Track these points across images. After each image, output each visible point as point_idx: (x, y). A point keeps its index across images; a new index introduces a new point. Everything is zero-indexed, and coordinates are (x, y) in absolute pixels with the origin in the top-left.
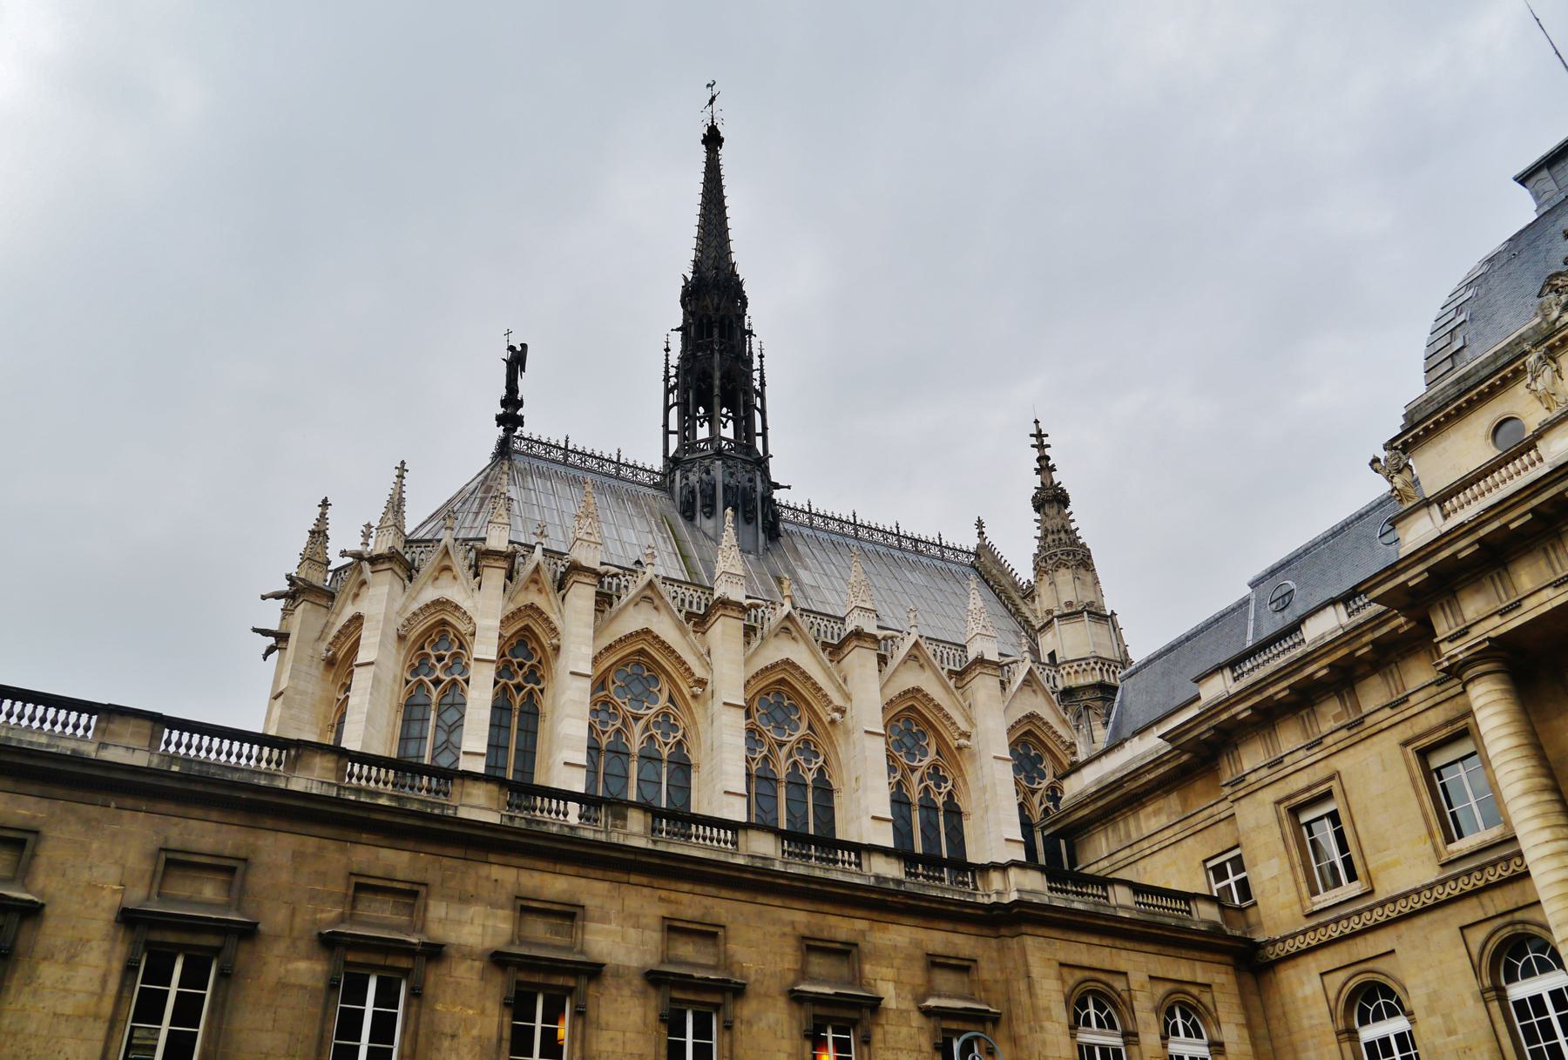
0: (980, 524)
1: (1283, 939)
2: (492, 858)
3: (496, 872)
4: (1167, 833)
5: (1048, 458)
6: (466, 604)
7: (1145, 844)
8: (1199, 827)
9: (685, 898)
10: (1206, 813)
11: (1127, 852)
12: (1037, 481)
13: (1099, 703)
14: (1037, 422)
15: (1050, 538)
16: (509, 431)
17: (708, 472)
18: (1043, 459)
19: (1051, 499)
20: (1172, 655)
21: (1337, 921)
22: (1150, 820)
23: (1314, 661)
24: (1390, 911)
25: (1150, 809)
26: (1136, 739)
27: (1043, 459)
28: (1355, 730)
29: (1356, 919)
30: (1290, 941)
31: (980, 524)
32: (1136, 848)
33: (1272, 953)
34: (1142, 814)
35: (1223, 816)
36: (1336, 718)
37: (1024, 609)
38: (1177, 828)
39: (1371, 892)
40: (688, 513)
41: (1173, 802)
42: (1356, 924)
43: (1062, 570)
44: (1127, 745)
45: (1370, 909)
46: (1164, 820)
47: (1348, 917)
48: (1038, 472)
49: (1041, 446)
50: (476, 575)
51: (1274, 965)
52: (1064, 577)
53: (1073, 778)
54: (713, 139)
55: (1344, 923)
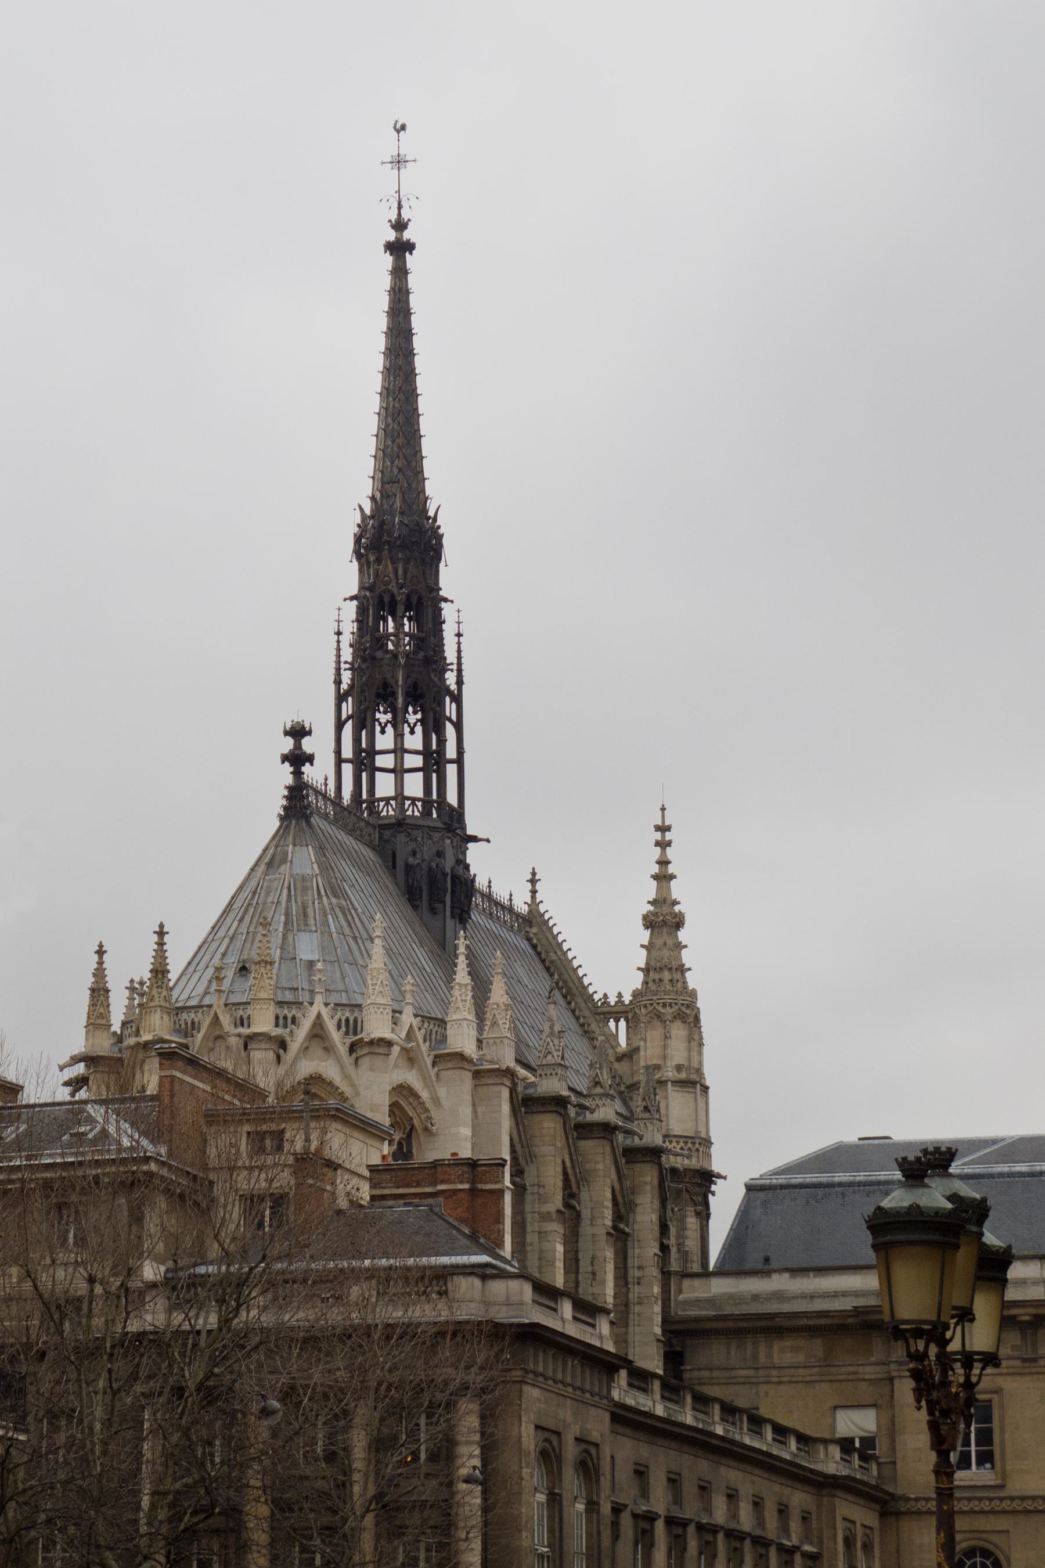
0: (533, 881)
1: (917, 1500)
2: (723, 1461)
3: (723, 1471)
4: (801, 1371)
5: (669, 862)
6: (425, 1095)
7: (774, 1372)
8: (840, 1377)
9: (756, 1479)
10: (851, 1369)
11: (752, 1372)
12: (651, 889)
13: (697, 1189)
14: (663, 809)
15: (666, 975)
16: (297, 773)
17: (440, 854)
18: (663, 863)
19: (664, 921)
20: (820, 1191)
21: (969, 1499)
22: (785, 1353)
23: (1023, 1307)
24: (1017, 1505)
25: (788, 1343)
26: (787, 1275)
27: (663, 863)
28: (1027, 1365)
29: (987, 1503)
30: (923, 1503)
31: (533, 881)
32: (761, 1372)
33: (902, 1506)
34: (777, 1345)
35: (867, 1377)
36: (1013, 1348)
37: (594, 1027)
38: (816, 1370)
39: (1002, 1487)
40: (412, 895)
41: (817, 1346)
42: (986, 1505)
43: (678, 1023)
44: (775, 1277)
45: (1001, 1499)
46: (800, 1358)
47: (980, 1499)
48: (655, 877)
49: (663, 845)
50: (434, 1064)
51: (897, 1514)
52: (678, 1031)
53: (697, 1282)
54: (400, 249)
55: (976, 1503)
